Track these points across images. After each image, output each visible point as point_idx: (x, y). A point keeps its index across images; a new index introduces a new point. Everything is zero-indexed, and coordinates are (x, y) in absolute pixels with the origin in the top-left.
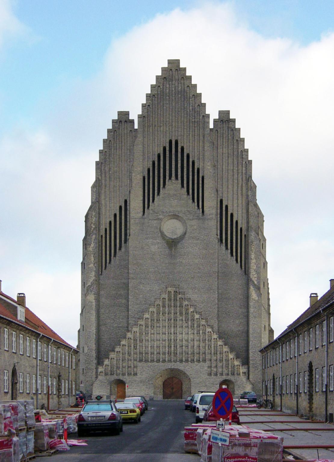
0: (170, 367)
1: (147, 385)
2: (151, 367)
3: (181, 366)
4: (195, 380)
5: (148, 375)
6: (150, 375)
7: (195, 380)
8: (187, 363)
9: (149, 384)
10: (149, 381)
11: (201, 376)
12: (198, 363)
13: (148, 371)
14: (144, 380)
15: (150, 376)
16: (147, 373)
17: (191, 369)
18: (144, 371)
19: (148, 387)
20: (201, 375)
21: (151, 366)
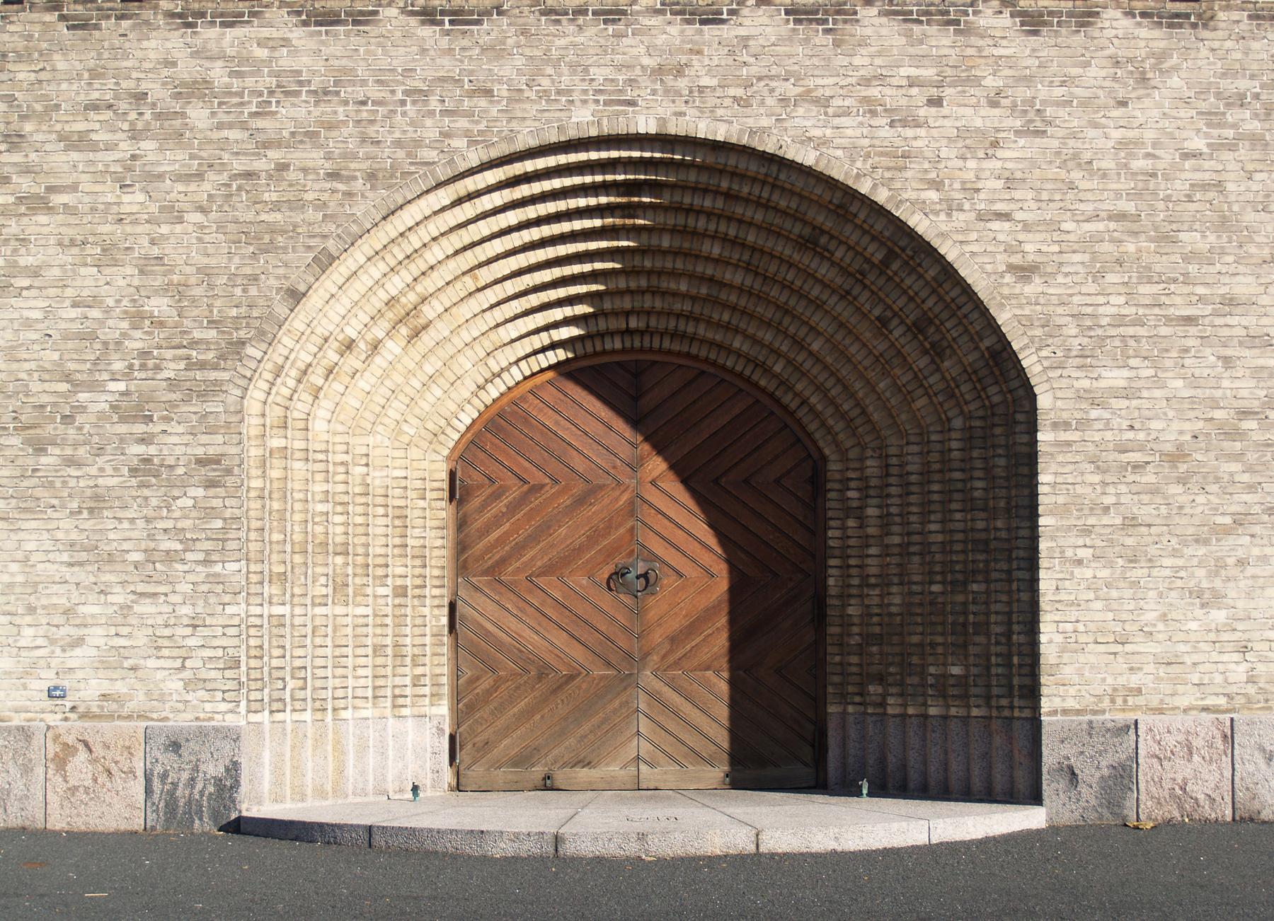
0: (584, 119)
1: (97, 503)
2: (198, 115)
3: (824, 84)
4: (1115, 377)
5: (124, 276)
6: (178, 291)
7: (1115, 377)
8: (941, 40)
9: (145, 469)
10: (134, 410)
11: (1231, 303)
12: (1149, 37)
13: (134, 200)
14: (46, 391)
15: (159, 306)
16: (110, 255)
17: (1015, 152)
18: (37, 204)
19: (123, 533)
20: (1244, 286)
21: (197, 90)
